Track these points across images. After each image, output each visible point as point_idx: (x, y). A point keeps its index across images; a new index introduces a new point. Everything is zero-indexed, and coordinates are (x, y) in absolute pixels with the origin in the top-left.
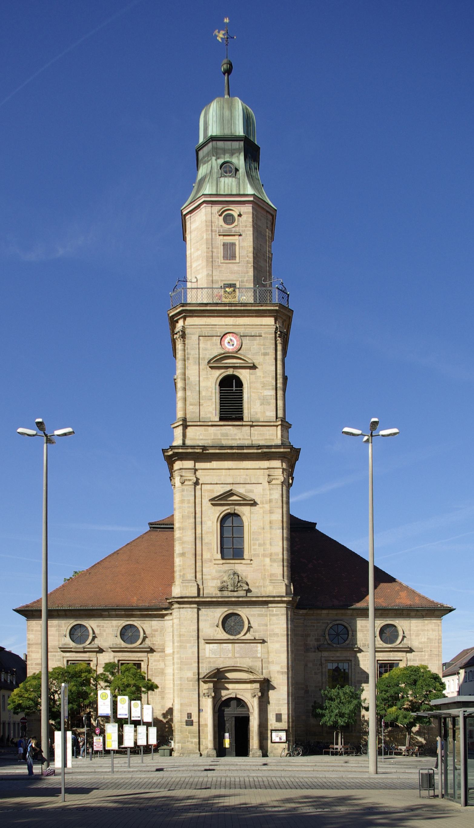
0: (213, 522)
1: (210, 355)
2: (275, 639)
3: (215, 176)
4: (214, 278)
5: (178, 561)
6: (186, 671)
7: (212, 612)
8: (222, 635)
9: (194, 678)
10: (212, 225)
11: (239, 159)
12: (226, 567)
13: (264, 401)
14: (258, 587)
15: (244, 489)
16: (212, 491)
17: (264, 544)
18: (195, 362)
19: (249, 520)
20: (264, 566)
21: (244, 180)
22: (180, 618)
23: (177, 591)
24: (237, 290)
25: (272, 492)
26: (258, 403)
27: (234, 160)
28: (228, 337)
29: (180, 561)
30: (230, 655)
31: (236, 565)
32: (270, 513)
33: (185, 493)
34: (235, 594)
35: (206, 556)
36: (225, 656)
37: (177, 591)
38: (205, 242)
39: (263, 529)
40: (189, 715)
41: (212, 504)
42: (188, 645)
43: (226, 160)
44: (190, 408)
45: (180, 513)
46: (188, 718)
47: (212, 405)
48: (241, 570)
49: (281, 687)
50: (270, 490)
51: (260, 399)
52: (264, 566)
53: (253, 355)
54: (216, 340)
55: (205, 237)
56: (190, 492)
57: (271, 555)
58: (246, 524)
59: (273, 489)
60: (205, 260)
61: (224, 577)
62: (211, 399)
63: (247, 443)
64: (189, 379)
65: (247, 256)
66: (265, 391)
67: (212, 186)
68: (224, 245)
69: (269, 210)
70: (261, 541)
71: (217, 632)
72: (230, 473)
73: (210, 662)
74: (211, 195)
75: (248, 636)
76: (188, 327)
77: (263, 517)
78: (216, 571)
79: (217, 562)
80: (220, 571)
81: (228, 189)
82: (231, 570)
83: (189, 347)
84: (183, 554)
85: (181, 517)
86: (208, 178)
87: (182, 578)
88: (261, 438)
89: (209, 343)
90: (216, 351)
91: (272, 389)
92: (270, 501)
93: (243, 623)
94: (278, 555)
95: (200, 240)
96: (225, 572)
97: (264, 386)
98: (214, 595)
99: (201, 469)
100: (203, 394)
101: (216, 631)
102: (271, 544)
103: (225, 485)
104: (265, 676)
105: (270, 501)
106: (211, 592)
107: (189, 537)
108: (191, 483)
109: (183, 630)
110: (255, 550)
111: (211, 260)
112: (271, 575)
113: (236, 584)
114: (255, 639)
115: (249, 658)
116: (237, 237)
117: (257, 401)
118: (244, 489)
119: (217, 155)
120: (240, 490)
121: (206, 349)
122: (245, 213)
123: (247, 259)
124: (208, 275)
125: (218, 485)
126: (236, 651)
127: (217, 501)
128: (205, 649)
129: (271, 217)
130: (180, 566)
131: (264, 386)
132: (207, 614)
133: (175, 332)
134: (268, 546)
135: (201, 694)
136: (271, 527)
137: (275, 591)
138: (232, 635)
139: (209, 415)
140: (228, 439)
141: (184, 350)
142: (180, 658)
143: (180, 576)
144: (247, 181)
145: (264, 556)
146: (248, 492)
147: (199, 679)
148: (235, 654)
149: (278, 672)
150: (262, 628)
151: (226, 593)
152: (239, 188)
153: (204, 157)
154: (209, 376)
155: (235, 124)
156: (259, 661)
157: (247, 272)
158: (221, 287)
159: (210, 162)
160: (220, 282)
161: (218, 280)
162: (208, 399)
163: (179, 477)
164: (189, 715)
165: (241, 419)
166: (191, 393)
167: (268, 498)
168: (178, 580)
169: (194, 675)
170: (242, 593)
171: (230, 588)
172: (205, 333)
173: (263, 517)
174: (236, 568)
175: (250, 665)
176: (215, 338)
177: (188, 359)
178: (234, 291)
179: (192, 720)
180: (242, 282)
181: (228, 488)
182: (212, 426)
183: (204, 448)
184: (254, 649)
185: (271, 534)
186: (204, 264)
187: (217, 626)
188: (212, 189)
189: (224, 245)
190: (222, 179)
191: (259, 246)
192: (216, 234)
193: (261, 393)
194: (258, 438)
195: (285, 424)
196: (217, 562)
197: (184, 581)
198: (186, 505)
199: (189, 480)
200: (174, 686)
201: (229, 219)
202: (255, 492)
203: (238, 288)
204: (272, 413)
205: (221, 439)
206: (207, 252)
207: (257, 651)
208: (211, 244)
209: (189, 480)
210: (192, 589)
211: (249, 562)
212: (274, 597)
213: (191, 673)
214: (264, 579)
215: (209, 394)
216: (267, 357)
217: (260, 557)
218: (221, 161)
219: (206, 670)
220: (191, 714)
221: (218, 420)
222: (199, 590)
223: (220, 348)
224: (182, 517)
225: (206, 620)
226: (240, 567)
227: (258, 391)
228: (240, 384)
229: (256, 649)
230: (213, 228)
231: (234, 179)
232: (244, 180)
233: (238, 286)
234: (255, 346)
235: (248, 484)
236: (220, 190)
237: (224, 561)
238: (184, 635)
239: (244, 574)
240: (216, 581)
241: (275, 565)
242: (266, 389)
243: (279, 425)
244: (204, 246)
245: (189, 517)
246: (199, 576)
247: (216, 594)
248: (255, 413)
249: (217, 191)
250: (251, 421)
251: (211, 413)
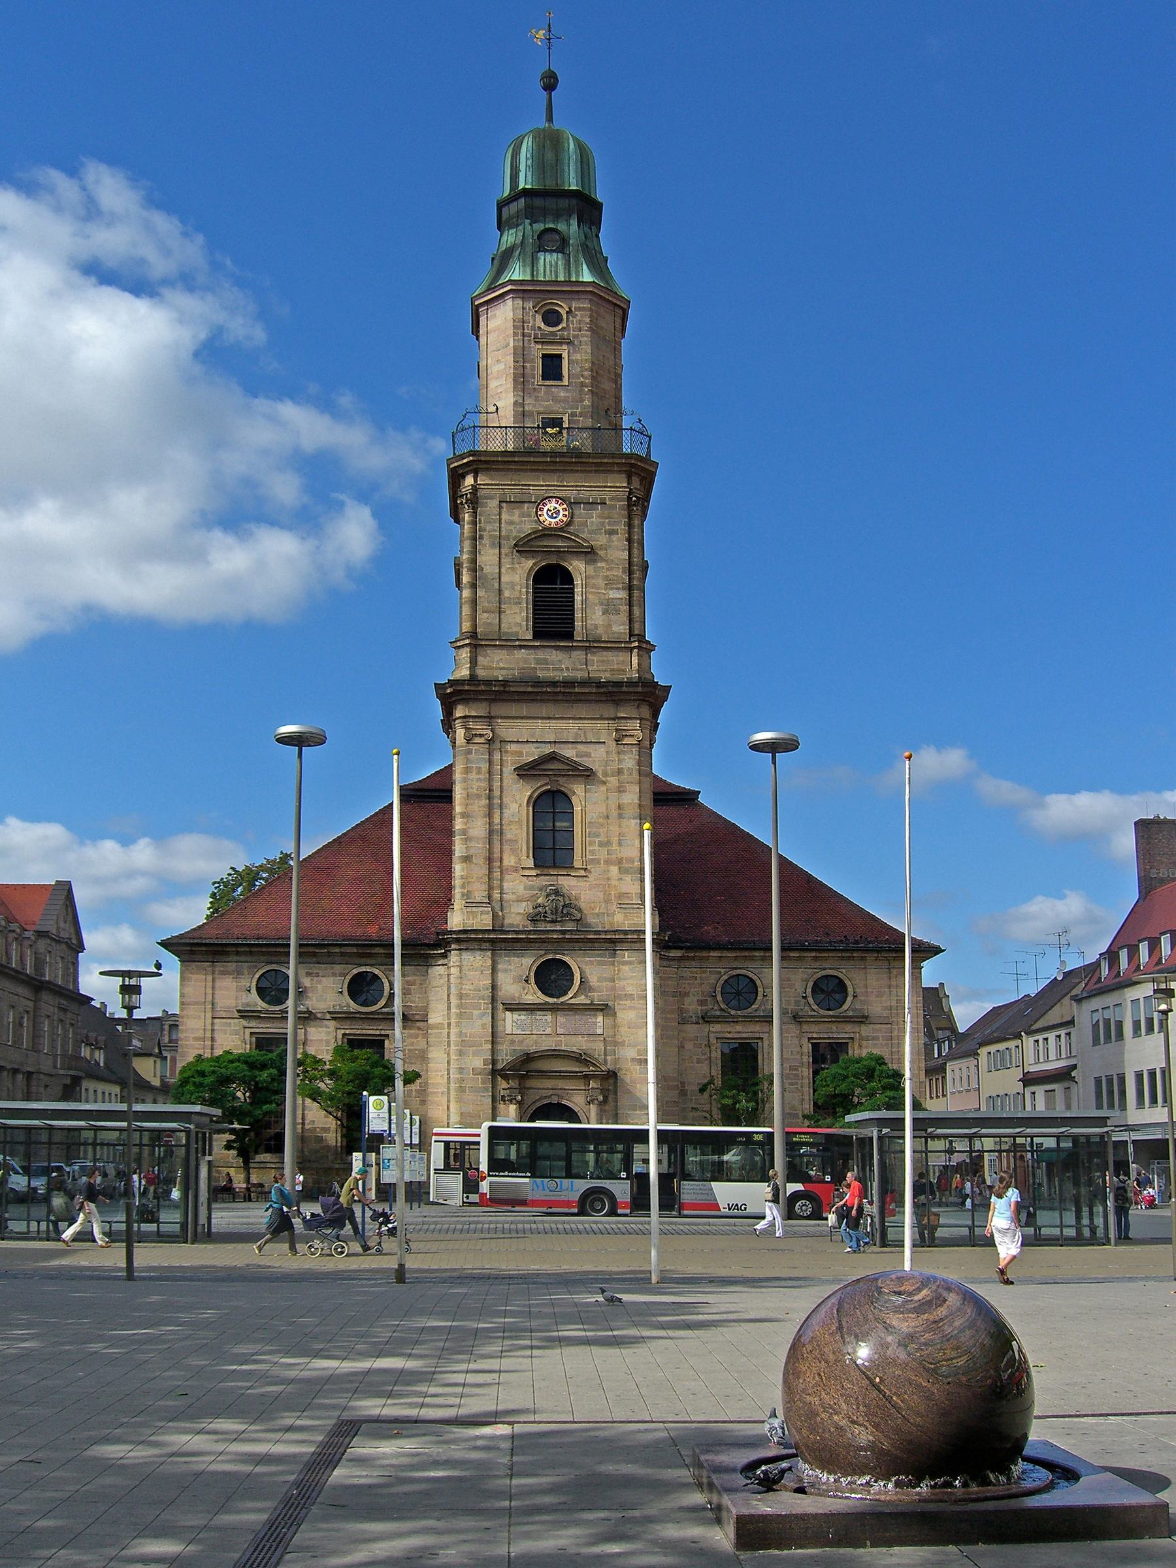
0: (520, 806)
1: (518, 532)
2: (628, 1003)
3: (529, 250)
4: (527, 408)
5: (458, 869)
8: (534, 995)
10: (523, 326)
11: (569, 225)
12: (544, 881)
13: (609, 607)
14: (598, 915)
15: (574, 752)
16: (520, 753)
17: (608, 843)
18: (493, 544)
19: (583, 803)
20: (609, 879)
21: (576, 257)
22: (460, 967)
23: (456, 920)
24: (565, 432)
25: (622, 757)
26: (598, 611)
27: (561, 227)
28: (552, 505)
29: (463, 869)
30: (549, 1031)
32: (620, 792)
33: (473, 756)
35: (509, 861)
37: (456, 920)
38: (512, 351)
39: (608, 817)
41: (518, 775)
42: (476, 1012)
43: (547, 226)
44: (482, 617)
45: (464, 789)
47: (520, 613)
48: (568, 886)
49: (638, 1086)
50: (619, 753)
51: (601, 604)
52: (609, 879)
53: (590, 534)
54: (528, 508)
55: (511, 345)
56: (482, 754)
57: (620, 861)
58: (577, 809)
59: (624, 752)
60: (511, 380)
61: (538, 898)
62: (520, 603)
63: (579, 675)
64: (482, 569)
65: (582, 376)
66: (611, 592)
67: (524, 266)
68: (544, 356)
69: (618, 303)
70: (603, 838)
71: (526, 991)
72: (552, 725)
73: (513, 1042)
74: (522, 282)
75: (582, 999)
76: (482, 487)
77: (608, 798)
78: (525, 888)
79: (527, 873)
80: (531, 888)
81: (551, 271)
82: (551, 885)
83: (482, 518)
84: (467, 859)
85: (465, 795)
86: (518, 252)
87: (465, 897)
88: (604, 668)
89: (517, 512)
90: (528, 527)
91: (623, 589)
92: (620, 772)
93: (572, 975)
94: (633, 862)
95: (504, 348)
96: (541, 890)
97: (609, 583)
98: (521, 928)
99: (502, 718)
100: (507, 594)
101: (524, 989)
102: (620, 844)
103: (543, 745)
104: (610, 1066)
105: (620, 772)
107: (479, 829)
108: (482, 740)
109: (467, 987)
110: (592, 852)
111: (521, 381)
112: (621, 896)
113: (560, 910)
114: (592, 1004)
116: (565, 347)
117: (596, 608)
118: (574, 752)
119: (532, 217)
120: (569, 752)
121: (511, 523)
122: (579, 309)
123: (582, 379)
124: (515, 403)
125: (531, 745)
127: (527, 770)
129: (620, 312)
130: (462, 877)
131: (609, 583)
133: (460, 494)
134: (615, 847)
135: (499, 1098)
136: (620, 816)
137: (626, 922)
138: (551, 996)
139: (515, 629)
140: (548, 669)
141: (474, 523)
142: (460, 1034)
143: (463, 894)
144: (581, 254)
145: (608, 862)
146: (582, 756)
147: (494, 1072)
148: (558, 1028)
149: (633, 1060)
150: (605, 984)
151: (542, 927)
152: (569, 271)
153: (510, 218)
154: (517, 566)
155: (563, 171)
156: (600, 1041)
157: (582, 401)
158: (538, 425)
159: (521, 228)
160: (535, 414)
161: (533, 412)
162: (516, 603)
163: (463, 731)
165: (569, 636)
166: (486, 592)
167: (614, 766)
168: (458, 903)
169: (484, 1065)
170: (570, 926)
171: (550, 917)
172: (510, 496)
173: (608, 798)
175: (584, 1048)
176: (526, 505)
177: (481, 537)
178: (560, 432)
180: (573, 415)
181: (548, 749)
182: (521, 647)
183: (505, 683)
185: (620, 826)
186: (510, 385)
187: (526, 981)
188: (524, 271)
189: (544, 356)
190: (541, 256)
191: (601, 358)
192: (529, 340)
193: (605, 594)
194: (600, 668)
195: (644, 646)
196: (527, 873)
197: (469, 903)
198: (473, 776)
199: (481, 735)
200: (449, 1083)
201: (552, 318)
202: (593, 755)
203: (567, 428)
204: (621, 627)
205: (536, 668)
206: (515, 368)
207: (595, 1023)
208: (521, 355)
209: (481, 735)
210: (484, 917)
211: (582, 873)
212: (625, 932)
213: (478, 1061)
214: (607, 901)
215: (517, 594)
216: (614, 538)
217: (602, 865)
218: (539, 227)
219: (507, 1055)
221: (529, 636)
222: (495, 916)
223: (536, 521)
224: (468, 796)
225: (506, 971)
226: (568, 883)
227: (599, 591)
228: (568, 578)
230: (526, 331)
231: (560, 255)
232: (576, 257)
233: (566, 425)
234: (594, 519)
236: (537, 273)
238: (467, 995)
239: (573, 893)
240: (524, 904)
241: (628, 878)
242: (612, 589)
243: (634, 647)
244: (510, 359)
245: (479, 796)
246: (496, 896)
247: (524, 926)
248: (593, 627)
249: (532, 275)
250: (587, 641)
251: (520, 625)
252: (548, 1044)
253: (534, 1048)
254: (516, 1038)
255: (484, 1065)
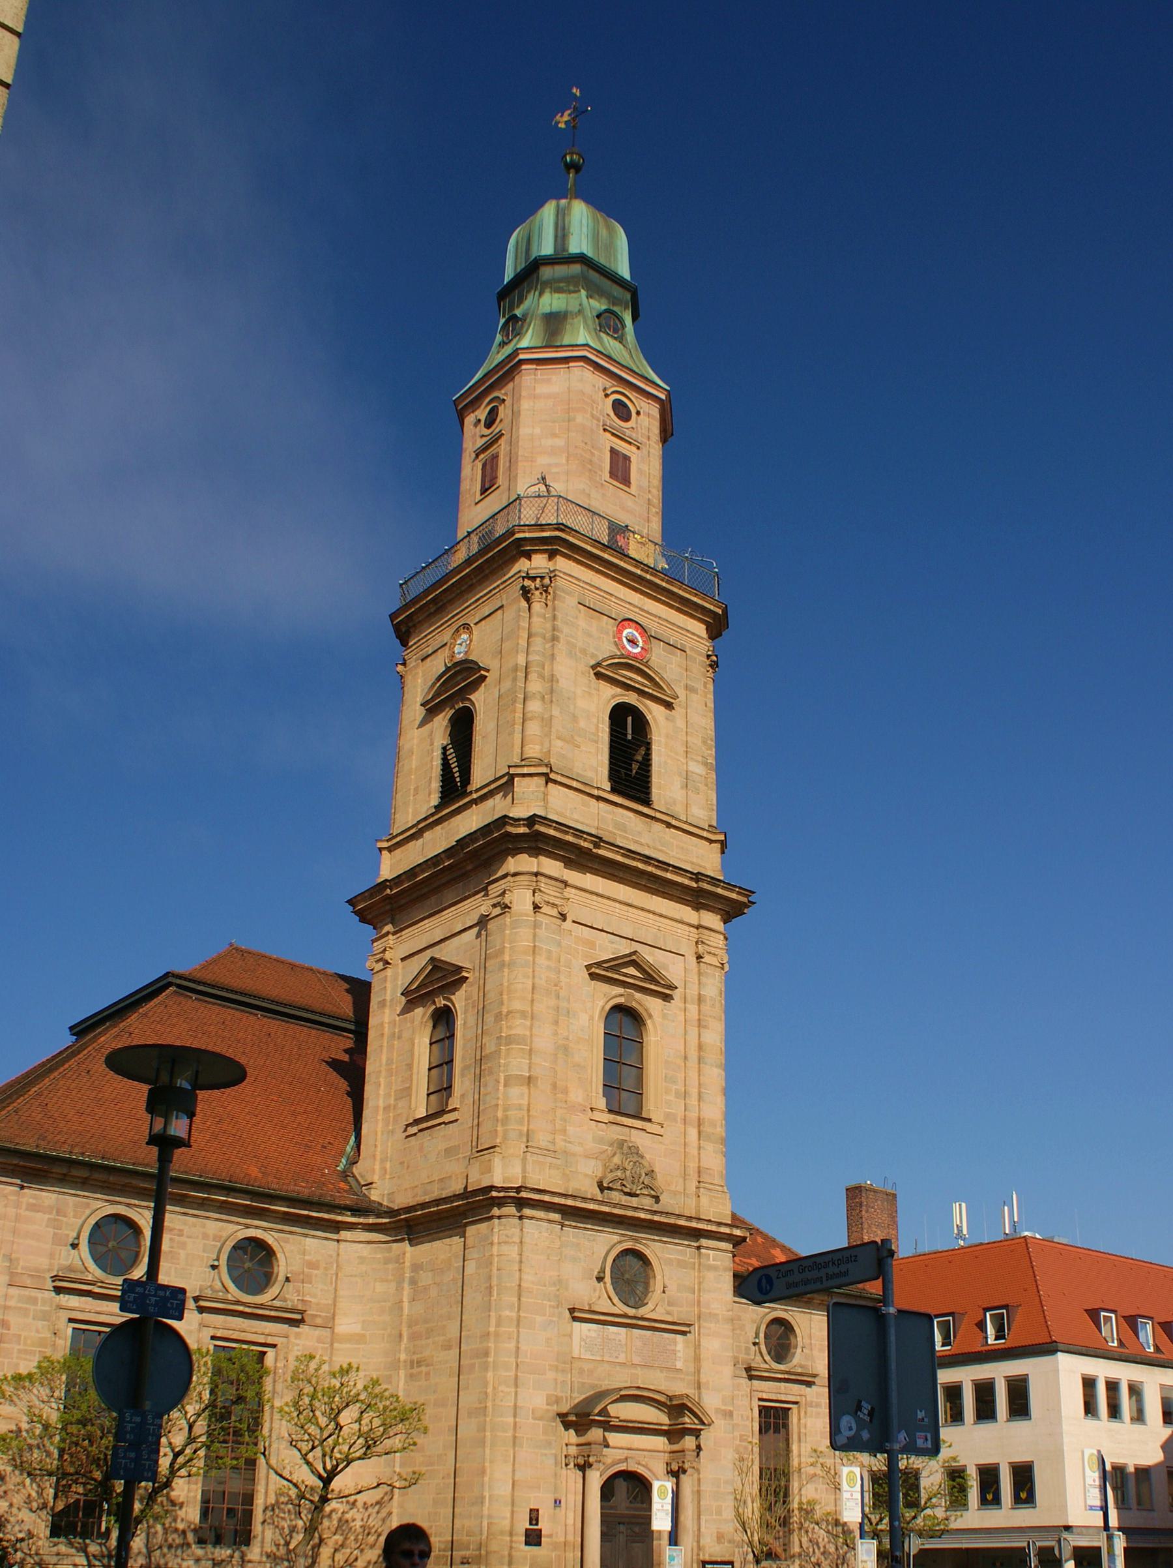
6: (530, 1391)
7: (589, 1240)
8: (604, 1299)
9: (548, 1410)
12: (616, 1133)
26: (677, 782)
31: (633, 1130)
34: (634, 1201)
36: (611, 1360)
40: (534, 1514)
42: (539, 1319)
46: (531, 1524)
73: (581, 1371)
101: (595, 1290)
106: (583, 1189)
115: (662, 1369)
126: (634, 1349)
128: (570, 1336)
132: (578, 1244)
151: (616, 1196)
164: (534, 1516)
169: (548, 1404)
170: (647, 1202)
174: (633, 1139)
179: (541, 1530)
184: (669, 1347)
207: (674, 1352)
220: (538, 1510)
227: (677, 757)
229: (673, 1348)
235: (660, 949)
237: (612, 1117)
252: (620, 1380)
253: (606, 1382)
254: (586, 1367)
255: (548, 1404)
